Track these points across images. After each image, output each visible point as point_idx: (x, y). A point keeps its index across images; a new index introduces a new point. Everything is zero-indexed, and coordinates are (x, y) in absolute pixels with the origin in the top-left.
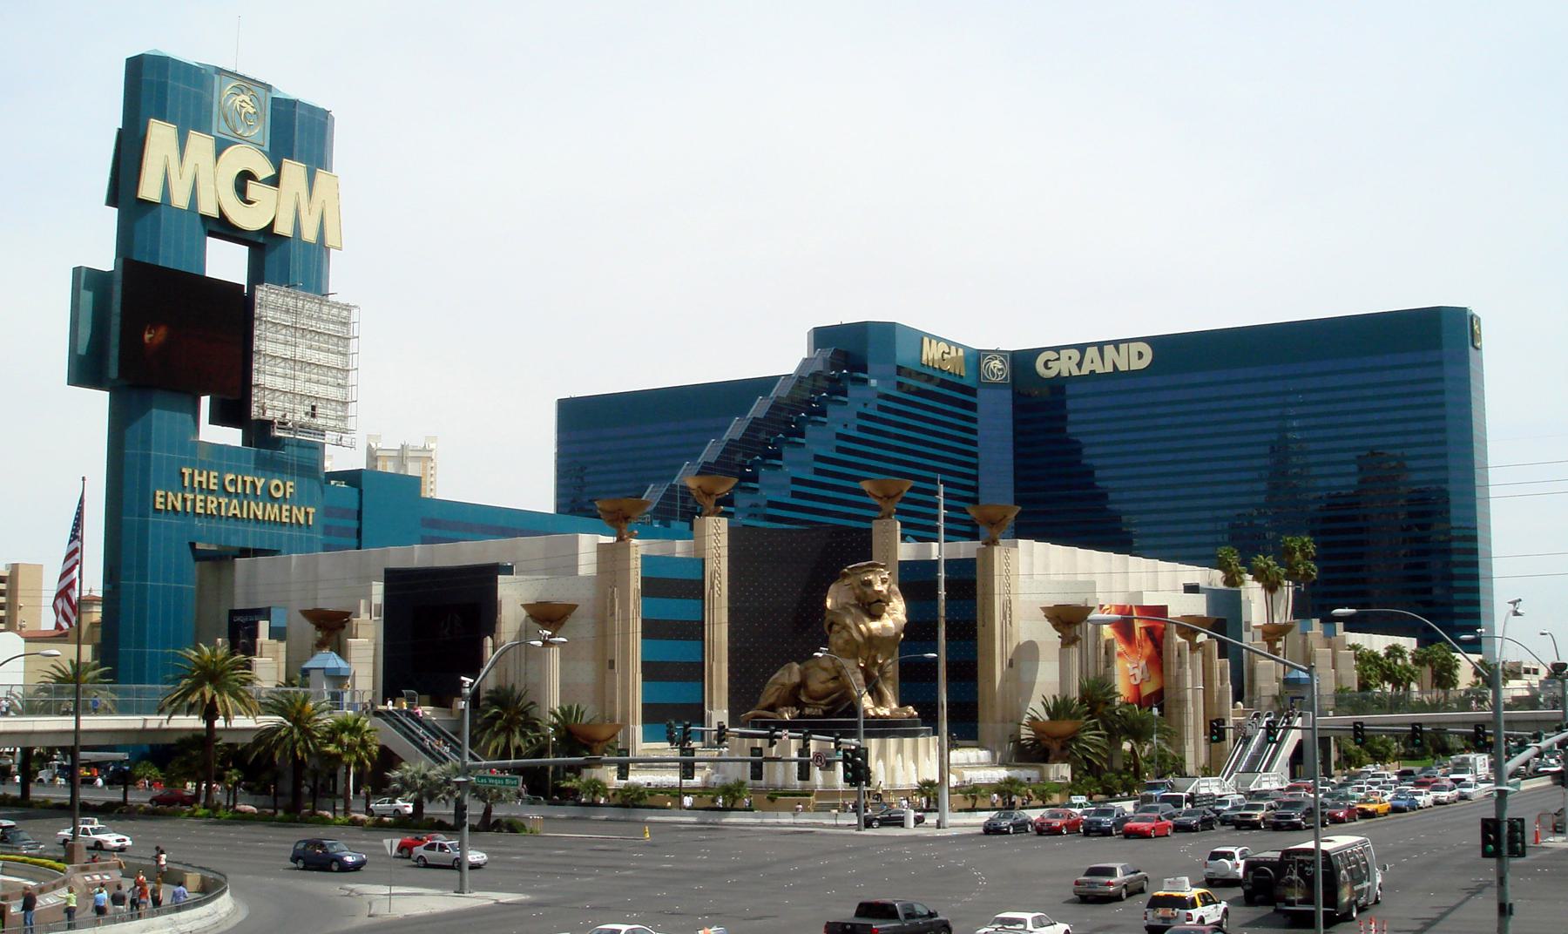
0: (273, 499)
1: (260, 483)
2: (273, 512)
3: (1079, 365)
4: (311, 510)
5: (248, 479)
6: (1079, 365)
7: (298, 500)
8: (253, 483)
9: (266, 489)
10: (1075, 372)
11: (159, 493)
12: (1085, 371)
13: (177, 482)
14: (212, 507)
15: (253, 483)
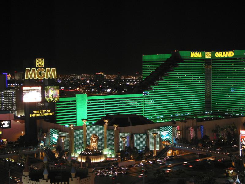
0: (47, 113)
1: (45, 111)
2: (47, 114)
3: (222, 55)
4: (53, 113)
5: (43, 111)
6: (222, 55)
7: (51, 112)
8: (44, 111)
9: (46, 111)
10: (221, 57)
11: (30, 115)
12: (223, 56)
13: (33, 113)
14: (38, 115)
15: (44, 111)
